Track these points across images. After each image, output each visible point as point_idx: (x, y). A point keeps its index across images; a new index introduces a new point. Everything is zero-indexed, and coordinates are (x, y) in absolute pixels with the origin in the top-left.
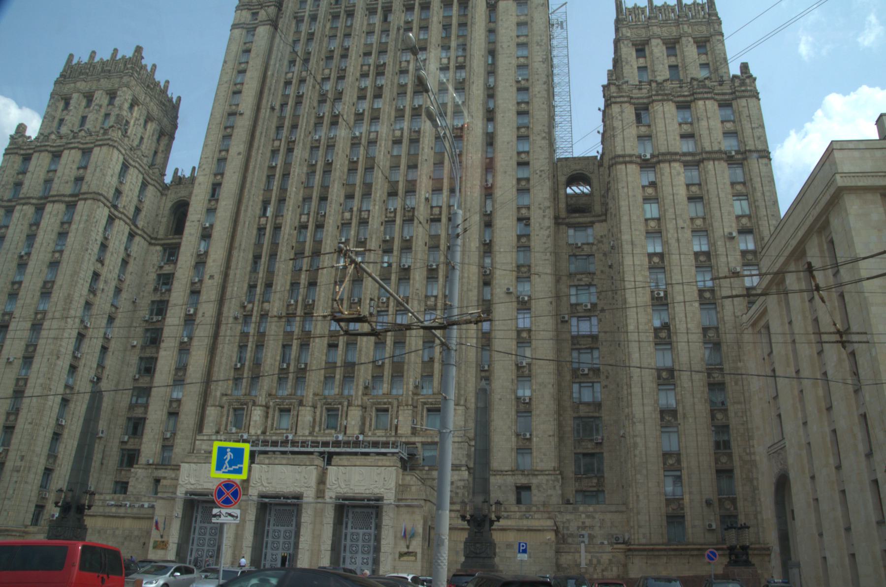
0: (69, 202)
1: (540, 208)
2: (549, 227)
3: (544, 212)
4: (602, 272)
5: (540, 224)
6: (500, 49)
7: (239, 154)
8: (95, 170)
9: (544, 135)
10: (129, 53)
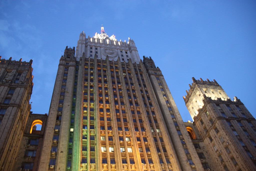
0: (3, 106)
1: (186, 136)
2: (191, 142)
3: (188, 137)
4: (208, 158)
5: (188, 141)
6: (156, 88)
7: (69, 105)
8: (18, 96)
9: (179, 114)
10: (28, 61)
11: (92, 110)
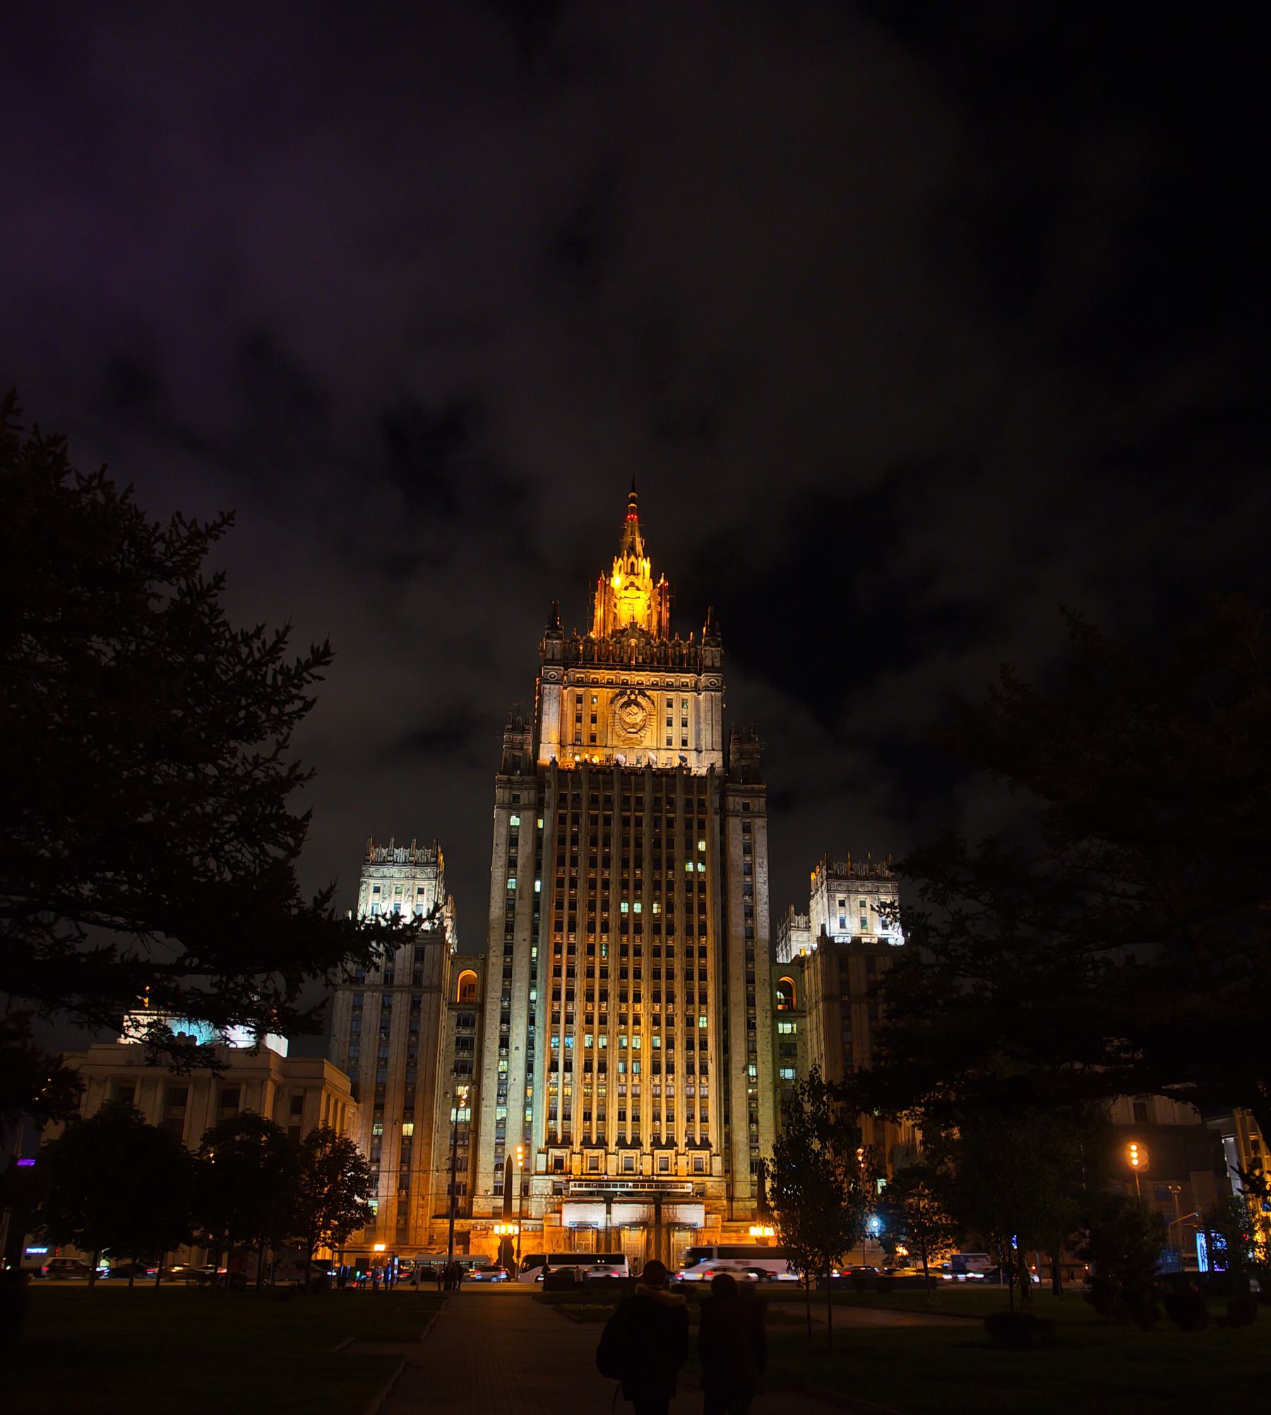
11: (572, 949)
